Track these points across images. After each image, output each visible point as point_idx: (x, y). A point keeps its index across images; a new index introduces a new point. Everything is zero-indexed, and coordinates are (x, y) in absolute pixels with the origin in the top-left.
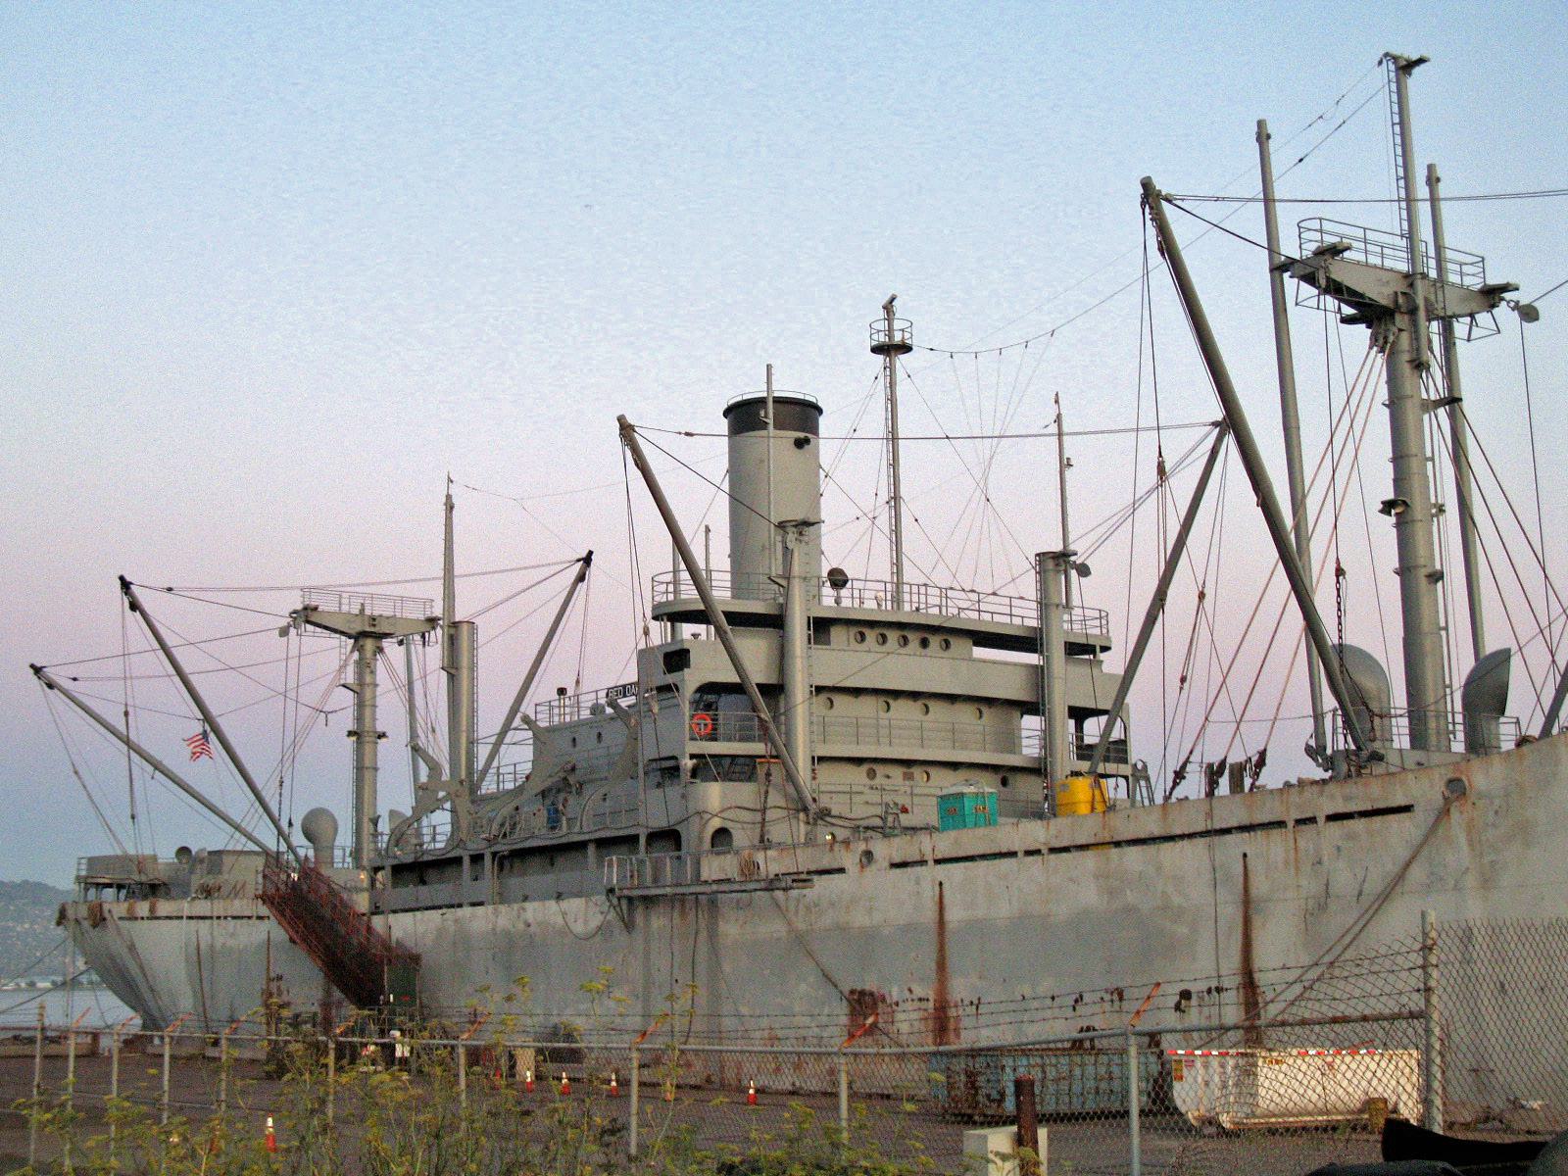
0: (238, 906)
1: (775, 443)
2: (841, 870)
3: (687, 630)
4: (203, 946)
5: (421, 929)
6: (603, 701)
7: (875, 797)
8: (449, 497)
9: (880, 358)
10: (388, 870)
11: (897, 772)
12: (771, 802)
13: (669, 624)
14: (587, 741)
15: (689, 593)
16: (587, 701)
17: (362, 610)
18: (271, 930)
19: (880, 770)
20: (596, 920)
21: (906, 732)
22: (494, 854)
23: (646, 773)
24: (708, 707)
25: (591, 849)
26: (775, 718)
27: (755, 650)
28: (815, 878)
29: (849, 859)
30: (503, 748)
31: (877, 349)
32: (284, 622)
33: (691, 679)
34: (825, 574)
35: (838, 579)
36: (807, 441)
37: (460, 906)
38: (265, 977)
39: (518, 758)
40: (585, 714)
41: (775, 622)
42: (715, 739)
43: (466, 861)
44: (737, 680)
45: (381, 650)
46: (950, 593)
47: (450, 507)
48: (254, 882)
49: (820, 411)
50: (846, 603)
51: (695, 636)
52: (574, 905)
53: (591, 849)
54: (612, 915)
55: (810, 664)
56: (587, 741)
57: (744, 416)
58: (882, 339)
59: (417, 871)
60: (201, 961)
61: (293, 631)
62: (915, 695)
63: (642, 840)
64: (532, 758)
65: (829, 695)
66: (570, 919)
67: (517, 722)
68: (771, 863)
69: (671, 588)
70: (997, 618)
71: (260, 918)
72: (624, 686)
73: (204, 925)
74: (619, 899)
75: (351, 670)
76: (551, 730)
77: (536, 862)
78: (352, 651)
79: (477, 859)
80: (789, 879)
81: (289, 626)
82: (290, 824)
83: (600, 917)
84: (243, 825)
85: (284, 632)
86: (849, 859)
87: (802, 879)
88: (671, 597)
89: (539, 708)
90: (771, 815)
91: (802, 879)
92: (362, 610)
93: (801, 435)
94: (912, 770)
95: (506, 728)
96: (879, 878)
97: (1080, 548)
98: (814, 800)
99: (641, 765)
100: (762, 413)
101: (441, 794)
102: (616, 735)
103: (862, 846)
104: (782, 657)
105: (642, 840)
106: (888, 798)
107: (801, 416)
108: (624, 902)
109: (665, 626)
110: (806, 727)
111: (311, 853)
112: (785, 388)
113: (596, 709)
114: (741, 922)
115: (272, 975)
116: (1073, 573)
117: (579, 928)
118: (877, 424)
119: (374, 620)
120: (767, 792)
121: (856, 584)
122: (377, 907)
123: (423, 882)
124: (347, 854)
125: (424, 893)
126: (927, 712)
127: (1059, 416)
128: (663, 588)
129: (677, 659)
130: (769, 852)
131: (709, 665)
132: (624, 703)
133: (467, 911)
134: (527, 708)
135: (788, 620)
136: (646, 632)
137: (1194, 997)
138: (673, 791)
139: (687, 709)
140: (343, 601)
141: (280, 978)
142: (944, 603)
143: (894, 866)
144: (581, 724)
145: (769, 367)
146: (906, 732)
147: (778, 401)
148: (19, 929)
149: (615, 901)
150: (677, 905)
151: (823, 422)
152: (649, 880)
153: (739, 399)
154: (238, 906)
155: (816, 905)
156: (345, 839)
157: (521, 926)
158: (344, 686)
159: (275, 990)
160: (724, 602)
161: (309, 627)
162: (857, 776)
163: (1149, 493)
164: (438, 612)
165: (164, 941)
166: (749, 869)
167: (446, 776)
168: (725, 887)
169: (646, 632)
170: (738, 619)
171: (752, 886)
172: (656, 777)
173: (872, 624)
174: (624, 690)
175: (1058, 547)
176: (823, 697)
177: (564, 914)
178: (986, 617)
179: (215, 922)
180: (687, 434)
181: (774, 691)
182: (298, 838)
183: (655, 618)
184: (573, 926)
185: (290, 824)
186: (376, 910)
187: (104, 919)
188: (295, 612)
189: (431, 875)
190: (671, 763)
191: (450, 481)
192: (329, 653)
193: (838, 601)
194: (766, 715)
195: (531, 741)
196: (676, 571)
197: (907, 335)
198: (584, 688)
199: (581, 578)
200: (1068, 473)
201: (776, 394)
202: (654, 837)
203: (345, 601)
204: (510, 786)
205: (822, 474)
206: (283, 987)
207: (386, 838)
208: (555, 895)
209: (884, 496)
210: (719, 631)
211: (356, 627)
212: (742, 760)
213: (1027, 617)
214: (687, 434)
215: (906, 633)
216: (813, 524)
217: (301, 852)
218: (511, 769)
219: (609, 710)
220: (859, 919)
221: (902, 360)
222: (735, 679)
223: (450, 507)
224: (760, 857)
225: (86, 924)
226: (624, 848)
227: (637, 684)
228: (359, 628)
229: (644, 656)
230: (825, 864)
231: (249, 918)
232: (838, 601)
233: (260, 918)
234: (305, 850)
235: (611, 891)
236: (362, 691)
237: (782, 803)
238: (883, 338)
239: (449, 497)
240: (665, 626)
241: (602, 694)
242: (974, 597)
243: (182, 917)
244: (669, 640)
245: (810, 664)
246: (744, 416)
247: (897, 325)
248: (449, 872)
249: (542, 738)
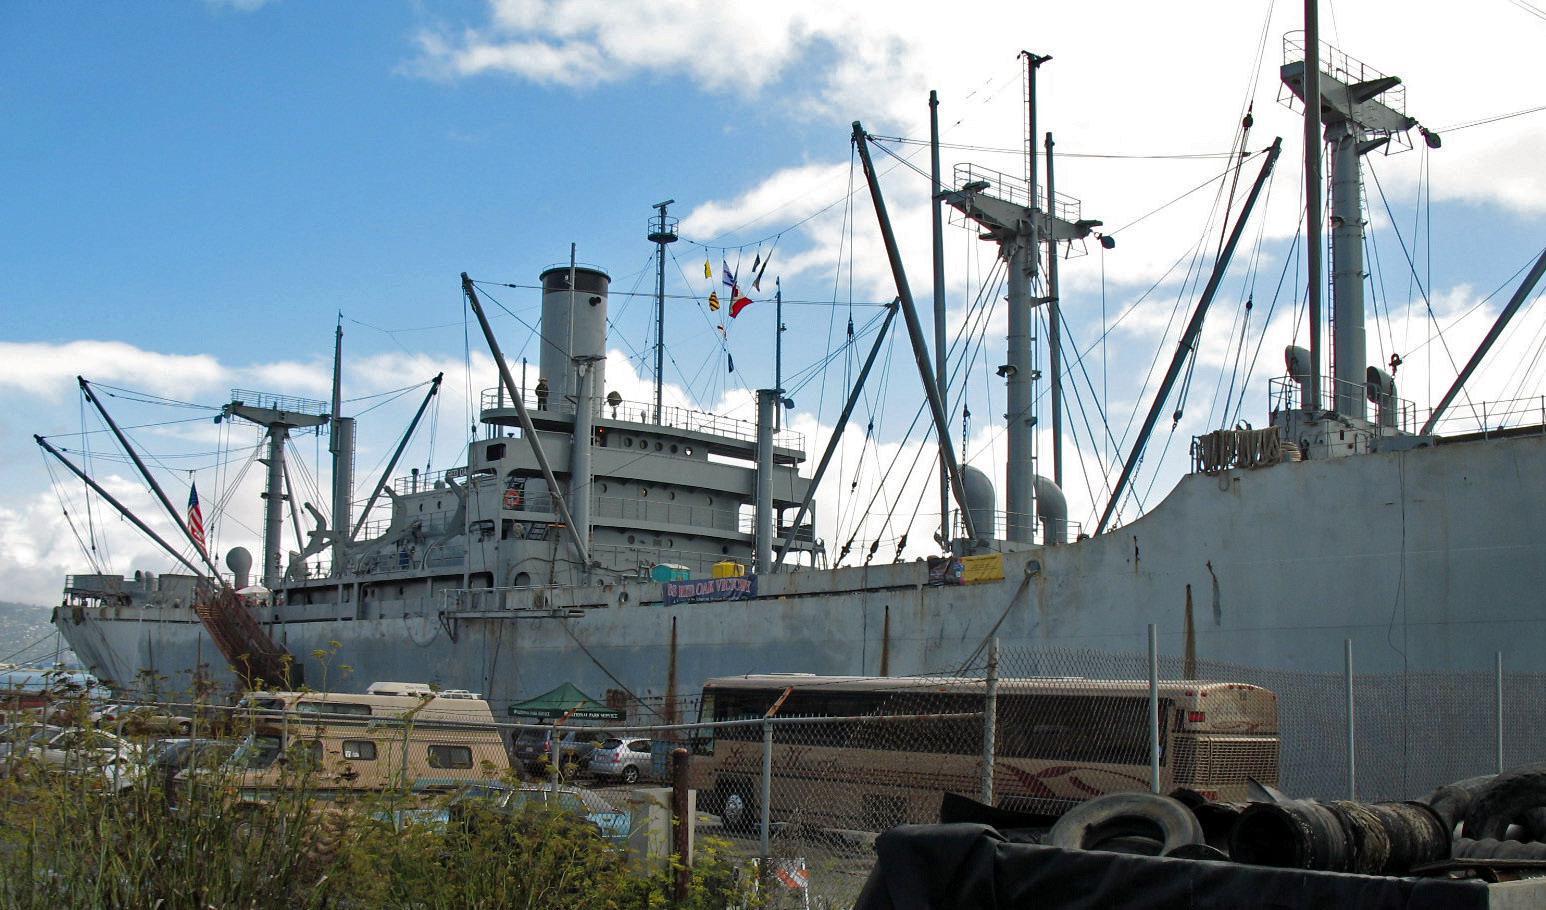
0: (178, 614)
1: (575, 298)
2: (605, 605)
3: (507, 430)
4: (153, 641)
5: (307, 636)
6: (443, 479)
7: (633, 556)
8: (339, 328)
9: (654, 244)
10: (285, 591)
11: (650, 539)
12: (558, 557)
13: (492, 425)
14: (430, 506)
15: (508, 403)
16: (433, 478)
17: (275, 407)
18: (199, 632)
19: (638, 537)
20: (430, 636)
21: (657, 514)
22: (360, 584)
23: (470, 531)
24: (517, 486)
25: (429, 583)
26: (566, 494)
27: (552, 449)
28: (586, 610)
29: (611, 599)
30: (373, 509)
31: (652, 238)
32: (218, 413)
33: (505, 465)
34: (606, 396)
35: (614, 399)
36: (598, 300)
37: (335, 620)
38: (196, 664)
39: (382, 518)
40: (431, 488)
41: (567, 428)
42: (522, 509)
43: (341, 587)
44: (539, 468)
45: (287, 436)
46: (694, 414)
47: (339, 335)
48: (190, 596)
49: (610, 281)
50: (619, 417)
51: (511, 435)
52: (416, 622)
53: (429, 583)
54: (442, 631)
55: (594, 460)
56: (430, 506)
57: (555, 280)
58: (656, 231)
59: (301, 592)
60: (151, 649)
61: (224, 420)
62: (665, 486)
63: (466, 578)
64: (391, 517)
65: (605, 483)
66: (413, 632)
67: (383, 491)
68: (558, 599)
69: (496, 400)
70: (727, 435)
71: (193, 622)
72: (459, 469)
73: (154, 626)
74: (448, 619)
75: (265, 448)
76: (406, 497)
77: (391, 591)
78: (267, 436)
79: (348, 587)
80: (567, 610)
81: (222, 415)
82: (217, 558)
83: (434, 632)
84: (184, 557)
85: (218, 420)
86: (611, 599)
87: (576, 611)
88: (495, 406)
89: (397, 482)
90: (558, 566)
91: (576, 611)
92: (275, 407)
93: (596, 296)
94: (660, 538)
95: (376, 494)
96: (631, 613)
97: (789, 389)
98: (590, 556)
99: (467, 526)
100: (567, 277)
101: (326, 540)
102: (451, 504)
103: (621, 589)
104: (572, 453)
105: (466, 578)
106: (642, 558)
107: (593, 282)
108: (452, 622)
109: (495, 428)
110: (589, 507)
111: (232, 580)
112: (582, 262)
113: (438, 485)
114: (533, 639)
115: (202, 663)
116: (782, 405)
117: (419, 639)
118: (650, 285)
119: (283, 414)
120: (556, 549)
121: (628, 405)
122: (277, 617)
123: (310, 602)
124: (259, 580)
125: (313, 610)
126: (673, 498)
127: (779, 293)
128: (489, 400)
129: (495, 451)
130: (555, 591)
131: (519, 457)
132: (459, 481)
133: (340, 624)
134: (389, 483)
135: (578, 429)
136: (474, 429)
137: (188, 605)
138: (489, 545)
139: (503, 488)
140: (262, 399)
141: (207, 666)
142: (690, 419)
143: (642, 604)
144: (425, 494)
145: (573, 245)
146: (657, 514)
147: (578, 271)
148: (31, 628)
149: (445, 621)
150: (489, 626)
151: (611, 287)
152: (469, 606)
153: (552, 268)
154: (178, 614)
155: (587, 630)
156: (257, 571)
157: (378, 636)
158: (260, 460)
159: (203, 674)
160: (531, 411)
161: (236, 417)
162: (622, 543)
163: (839, 350)
164: (329, 411)
165: (128, 637)
166: (539, 602)
167: (329, 528)
168: (522, 614)
169: (474, 429)
170: (541, 424)
171: (540, 614)
172: (477, 535)
173: (637, 434)
174: (459, 472)
175: (772, 386)
176: (601, 482)
177: (409, 629)
178: (720, 433)
179: (162, 624)
180: (511, 286)
181: (565, 477)
182: (223, 568)
183: (482, 421)
184: (414, 637)
185: (217, 558)
186: (277, 620)
187: (84, 619)
188: (227, 406)
189: (316, 596)
190: (490, 525)
191: (341, 316)
192: (248, 436)
193: (614, 415)
194: (558, 493)
195: (391, 506)
196: (500, 389)
197: (674, 229)
198: (432, 469)
199: (434, 391)
200: (782, 334)
201: (579, 266)
202: (474, 576)
203: (263, 400)
204: (374, 537)
205: (608, 325)
206: (210, 673)
207: (284, 570)
208: (402, 615)
209: (652, 342)
210: (528, 433)
211: (271, 419)
212: (539, 525)
213: (749, 434)
214: (511, 286)
215: (661, 441)
216: (599, 360)
217: (224, 578)
218: (376, 524)
219: (447, 486)
220: (615, 640)
221: (669, 246)
222: (537, 467)
223: (339, 335)
224: (547, 594)
225: (71, 622)
226: (453, 584)
227: (467, 468)
228: (272, 420)
229: (473, 446)
230: (594, 601)
231: (187, 622)
232: (614, 415)
233: (193, 622)
234: (230, 578)
235: (442, 613)
236: (275, 465)
237: (565, 557)
238: (657, 230)
239: (339, 328)
240: (495, 428)
241: (443, 474)
242: (711, 418)
243: (138, 620)
244: (492, 437)
245: (594, 460)
246: (555, 280)
247: (668, 221)
248: (331, 595)
249: (399, 503)
